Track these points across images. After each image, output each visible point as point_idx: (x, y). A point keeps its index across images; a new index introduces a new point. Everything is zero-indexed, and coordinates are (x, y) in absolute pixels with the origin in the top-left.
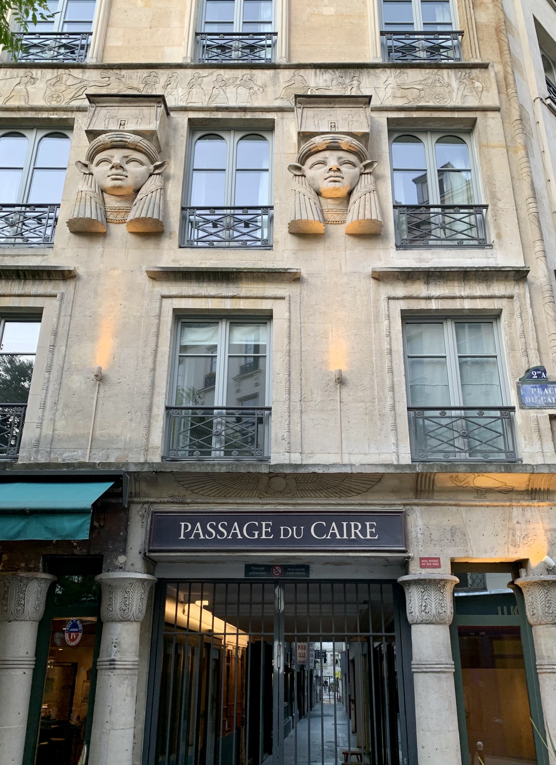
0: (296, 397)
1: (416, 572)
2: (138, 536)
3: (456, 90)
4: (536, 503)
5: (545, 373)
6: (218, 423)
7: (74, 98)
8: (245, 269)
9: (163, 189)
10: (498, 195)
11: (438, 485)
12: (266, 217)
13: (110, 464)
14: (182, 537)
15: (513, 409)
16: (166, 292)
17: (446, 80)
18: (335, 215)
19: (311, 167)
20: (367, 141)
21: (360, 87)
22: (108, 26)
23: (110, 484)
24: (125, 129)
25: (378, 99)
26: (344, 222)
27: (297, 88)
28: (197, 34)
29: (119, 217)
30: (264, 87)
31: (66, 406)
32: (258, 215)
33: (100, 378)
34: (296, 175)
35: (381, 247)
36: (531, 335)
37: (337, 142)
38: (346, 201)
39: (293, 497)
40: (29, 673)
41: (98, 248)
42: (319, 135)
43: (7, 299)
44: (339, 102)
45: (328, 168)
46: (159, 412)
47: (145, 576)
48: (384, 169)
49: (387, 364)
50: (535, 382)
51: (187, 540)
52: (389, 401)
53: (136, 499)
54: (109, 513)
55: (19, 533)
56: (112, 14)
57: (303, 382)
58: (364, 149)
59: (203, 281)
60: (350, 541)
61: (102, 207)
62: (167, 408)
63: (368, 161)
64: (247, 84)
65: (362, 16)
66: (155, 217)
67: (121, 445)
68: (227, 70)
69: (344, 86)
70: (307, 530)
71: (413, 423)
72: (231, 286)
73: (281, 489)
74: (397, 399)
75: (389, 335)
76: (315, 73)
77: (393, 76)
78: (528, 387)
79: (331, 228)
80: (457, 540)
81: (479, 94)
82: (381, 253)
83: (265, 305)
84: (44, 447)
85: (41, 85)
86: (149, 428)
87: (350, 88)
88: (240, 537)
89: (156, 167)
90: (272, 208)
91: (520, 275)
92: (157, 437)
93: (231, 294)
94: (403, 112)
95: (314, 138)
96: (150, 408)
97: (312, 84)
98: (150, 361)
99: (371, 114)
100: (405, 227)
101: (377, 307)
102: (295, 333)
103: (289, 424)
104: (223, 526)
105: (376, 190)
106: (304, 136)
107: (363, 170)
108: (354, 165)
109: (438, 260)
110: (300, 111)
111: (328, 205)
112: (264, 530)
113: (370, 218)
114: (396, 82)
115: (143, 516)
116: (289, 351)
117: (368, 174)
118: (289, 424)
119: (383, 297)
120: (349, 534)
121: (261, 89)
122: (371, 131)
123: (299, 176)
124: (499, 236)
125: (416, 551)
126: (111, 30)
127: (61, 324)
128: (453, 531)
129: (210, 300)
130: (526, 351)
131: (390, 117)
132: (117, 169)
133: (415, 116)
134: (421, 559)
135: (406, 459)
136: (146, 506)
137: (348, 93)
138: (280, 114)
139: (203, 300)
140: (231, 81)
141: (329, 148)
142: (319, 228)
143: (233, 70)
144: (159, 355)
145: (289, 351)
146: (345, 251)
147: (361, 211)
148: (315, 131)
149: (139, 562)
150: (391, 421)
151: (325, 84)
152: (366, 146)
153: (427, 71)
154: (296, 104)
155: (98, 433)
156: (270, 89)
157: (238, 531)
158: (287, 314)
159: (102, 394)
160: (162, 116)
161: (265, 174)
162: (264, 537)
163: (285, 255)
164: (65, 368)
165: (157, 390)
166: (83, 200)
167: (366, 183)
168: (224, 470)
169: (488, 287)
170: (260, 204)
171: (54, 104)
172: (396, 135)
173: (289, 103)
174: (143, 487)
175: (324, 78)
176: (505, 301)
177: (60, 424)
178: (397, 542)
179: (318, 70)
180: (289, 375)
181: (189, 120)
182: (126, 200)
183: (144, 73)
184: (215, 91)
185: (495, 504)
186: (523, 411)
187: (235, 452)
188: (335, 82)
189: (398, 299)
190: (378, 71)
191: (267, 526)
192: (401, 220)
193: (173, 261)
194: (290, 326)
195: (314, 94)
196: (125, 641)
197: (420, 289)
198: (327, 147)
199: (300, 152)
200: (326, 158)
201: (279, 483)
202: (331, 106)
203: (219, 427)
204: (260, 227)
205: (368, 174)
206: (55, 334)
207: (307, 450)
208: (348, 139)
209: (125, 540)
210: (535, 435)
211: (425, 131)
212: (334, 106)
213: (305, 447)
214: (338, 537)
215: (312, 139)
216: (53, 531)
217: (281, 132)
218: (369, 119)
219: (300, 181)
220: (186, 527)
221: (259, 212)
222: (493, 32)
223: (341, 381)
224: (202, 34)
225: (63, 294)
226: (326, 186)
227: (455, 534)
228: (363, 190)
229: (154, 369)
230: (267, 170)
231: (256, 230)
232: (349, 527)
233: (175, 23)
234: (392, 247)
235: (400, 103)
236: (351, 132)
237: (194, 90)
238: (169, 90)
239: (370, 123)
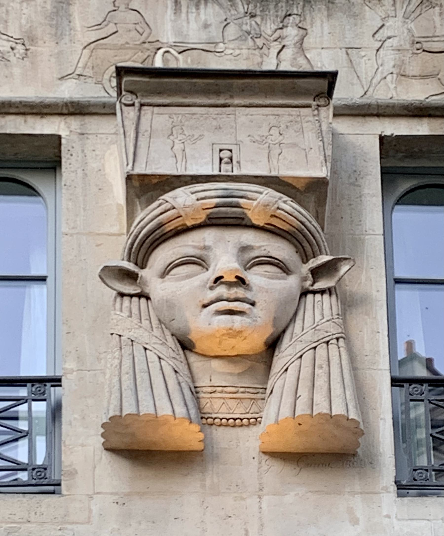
12: (40, 408)
20: (321, 202)
21: (305, 45)
25: (356, 81)
27: (122, 47)
32: (19, 401)
34: (122, 295)
37: (238, 206)
38: (261, 367)
42: (186, 184)
44: (243, 91)
45: (211, 275)
48: (368, 278)
58: (313, 225)
63: (324, 259)
69: (259, 42)
77: (400, 14)
79: (221, 435)
82: (358, 504)
87: (276, 47)
90: (56, 381)
94: (425, 121)
95: (171, 194)
97: (167, 36)
99: (334, 125)
100: (422, 434)
105: (344, 337)
106: (145, 187)
107: (309, 283)
108: (284, 269)
110: (131, 113)
111: (213, 375)
113: (326, 411)
114: (409, 30)
117: (322, 292)
121: (20, 49)
122: (334, 171)
123: (131, 296)
137: (270, 65)
138: (75, 123)
141: (214, 221)
142: (189, 436)
146: (260, 497)
147: (304, 393)
148: (175, 173)
151: (204, 36)
152: (319, 217)
154: (119, 93)
161: (36, 289)
163: (94, 508)
167: (318, 317)
170: (24, 373)
172: (405, 185)
173: (101, 90)
175: (203, 17)
192: (412, 415)
195: (173, 65)
198: (209, 217)
199: (134, 230)
200: (205, 248)
202: (221, 101)
204: (25, 435)
205: (322, 292)
208: (268, 195)
212: (229, 101)
215: (167, 196)
217: (80, 171)
218: (328, 138)
219: (135, 311)
221: (23, 392)
226: (205, 325)
228: (310, 337)
230: (42, 279)
231: (16, 440)
234: (386, 489)
236: (277, 177)
239: (329, 153)
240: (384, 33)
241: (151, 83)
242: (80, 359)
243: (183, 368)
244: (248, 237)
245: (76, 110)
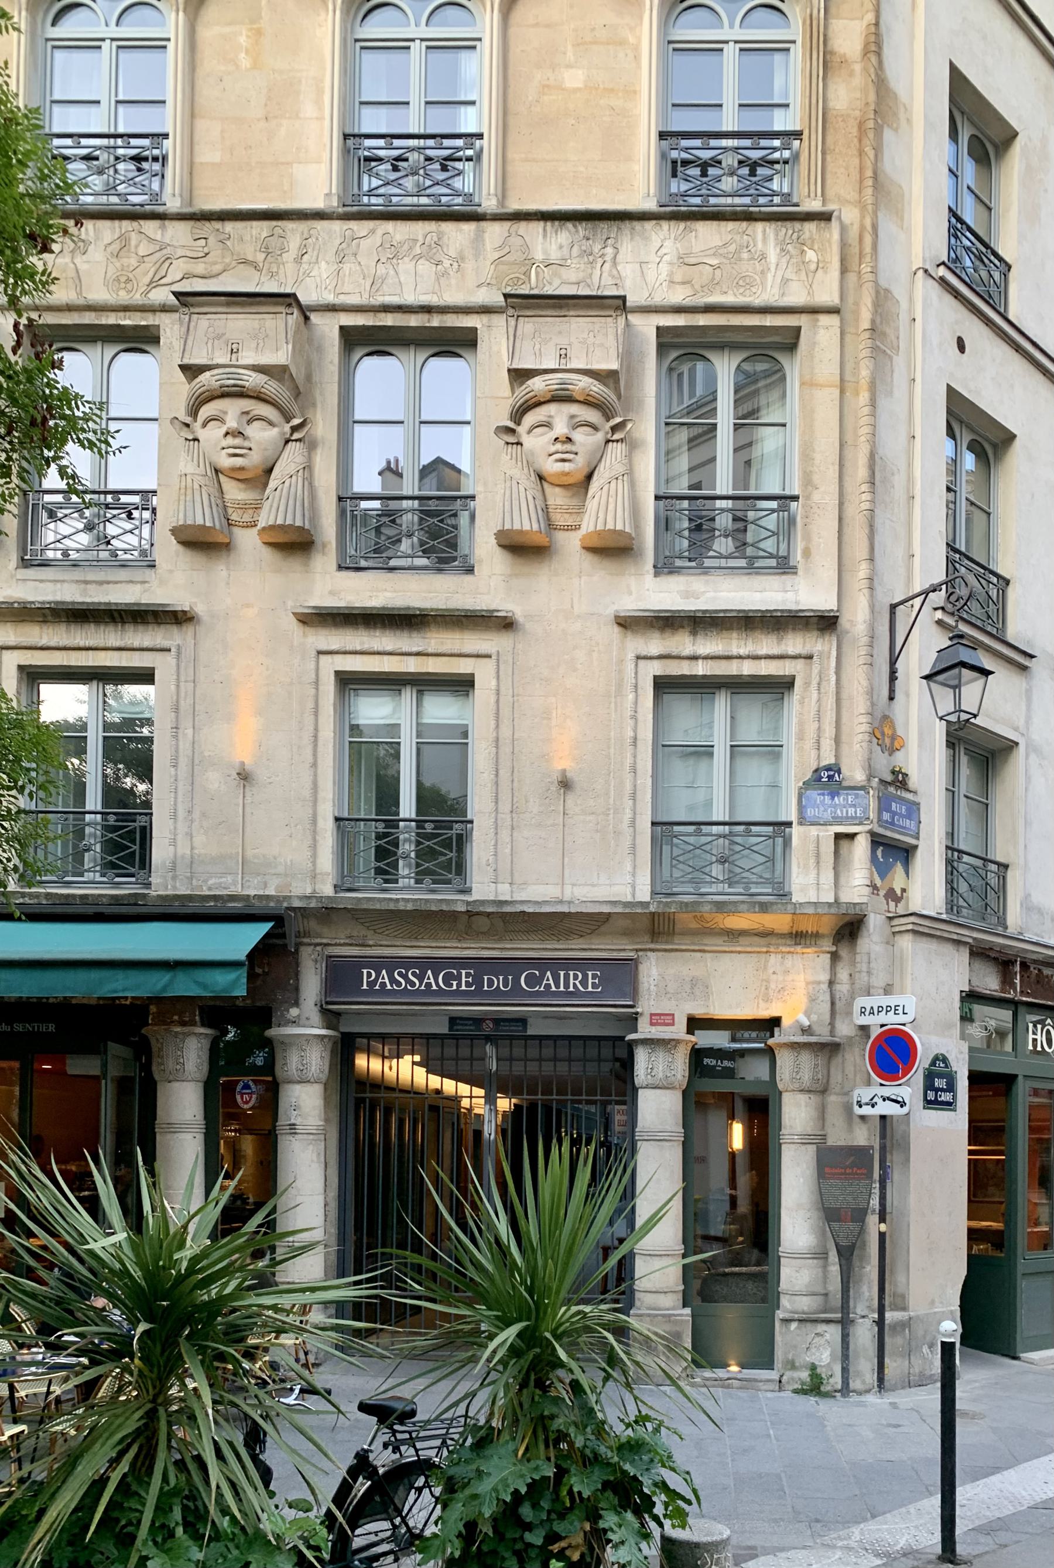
0: (505, 807)
1: (645, 1030)
2: (312, 985)
3: (773, 268)
4: (799, 949)
5: (839, 773)
6: (405, 840)
7: (153, 284)
8: (432, 610)
9: (308, 468)
10: (816, 478)
11: (678, 927)
13: (268, 897)
14: (365, 987)
15: (789, 824)
16: (324, 647)
17: (760, 245)
18: (567, 516)
22: (193, 116)
23: (270, 925)
24: (241, 362)
26: (577, 528)
27: (514, 263)
28: (346, 137)
29: (247, 518)
30: (460, 259)
31: (203, 815)
33: (245, 777)
35: (633, 571)
36: (829, 717)
39: (500, 940)
40: (200, 1138)
41: (220, 570)
43: (102, 654)
46: (327, 826)
47: (323, 1032)
49: (629, 761)
51: (371, 991)
52: (628, 814)
53: (306, 940)
54: (274, 958)
55: (165, 988)
56: (197, 88)
57: (516, 784)
59: (375, 627)
60: (568, 994)
61: (219, 501)
62: (337, 819)
64: (432, 253)
65: (631, 93)
66: (298, 523)
67: (281, 869)
68: (399, 223)
69: (591, 258)
70: (516, 981)
71: (656, 843)
72: (415, 634)
73: (485, 929)
74: (638, 811)
75: (634, 717)
76: (545, 230)
78: (813, 794)
80: (697, 992)
81: (811, 275)
82: (632, 582)
83: (462, 667)
84: (182, 871)
85: (96, 254)
86: (314, 847)
87: (600, 261)
88: (434, 987)
89: (294, 429)
91: (826, 623)
92: (327, 861)
93: (415, 649)
96: (314, 821)
98: (308, 751)
101: (620, 672)
102: (505, 711)
103: (496, 845)
104: (414, 974)
109: (712, 594)
111: (557, 498)
112: (464, 979)
115: (316, 961)
116: (497, 740)
118: (496, 845)
119: (631, 656)
120: (567, 986)
121: (455, 265)
124: (807, 553)
125: (647, 1005)
126: (201, 124)
127: (182, 695)
128: (694, 982)
129: (386, 658)
130: (818, 742)
132: (234, 436)
133: (701, 323)
134: (652, 1015)
135: (644, 894)
136: (319, 948)
138: (485, 318)
139: (377, 657)
140: (406, 247)
142: (542, 540)
143: (409, 223)
144: (320, 743)
145: (497, 740)
149: (315, 1016)
150: (627, 842)
151: (559, 255)
153: (731, 225)
155: (249, 853)
156: (469, 266)
157: (432, 980)
158: (494, 682)
159: (248, 800)
160: (297, 332)
162: (463, 988)
164: (196, 762)
165: (321, 794)
166: (189, 492)
168: (410, 907)
169: (780, 640)
171: (123, 297)
174: (313, 925)
177: (199, 839)
178: (624, 996)
179: (549, 224)
180: (497, 775)
181: (342, 328)
182: (255, 487)
183: (260, 228)
184: (381, 270)
185: (749, 949)
186: (802, 828)
187: (427, 880)
188: (575, 251)
189: (651, 658)
190: (649, 225)
191: (468, 975)
193: (332, 593)
194: (498, 701)
196: (306, 1104)
197: (684, 643)
201: (483, 923)
203: (407, 846)
206: (176, 709)
207: (518, 879)
209: (297, 989)
210: (812, 861)
211: (719, 347)
213: (516, 874)
214: (554, 989)
216: (205, 987)
220: (369, 975)
222: (855, 131)
223: (566, 784)
224: (354, 136)
225: (179, 647)
226: (551, 467)
227: (697, 986)
229: (314, 765)
232: (567, 977)
233: (309, 110)
235: (679, 296)
237: (346, 267)
238: (305, 266)
240: (663, 251)
241: (524, 303)
242: (485, 484)
243: (539, 495)
245: (486, 310)
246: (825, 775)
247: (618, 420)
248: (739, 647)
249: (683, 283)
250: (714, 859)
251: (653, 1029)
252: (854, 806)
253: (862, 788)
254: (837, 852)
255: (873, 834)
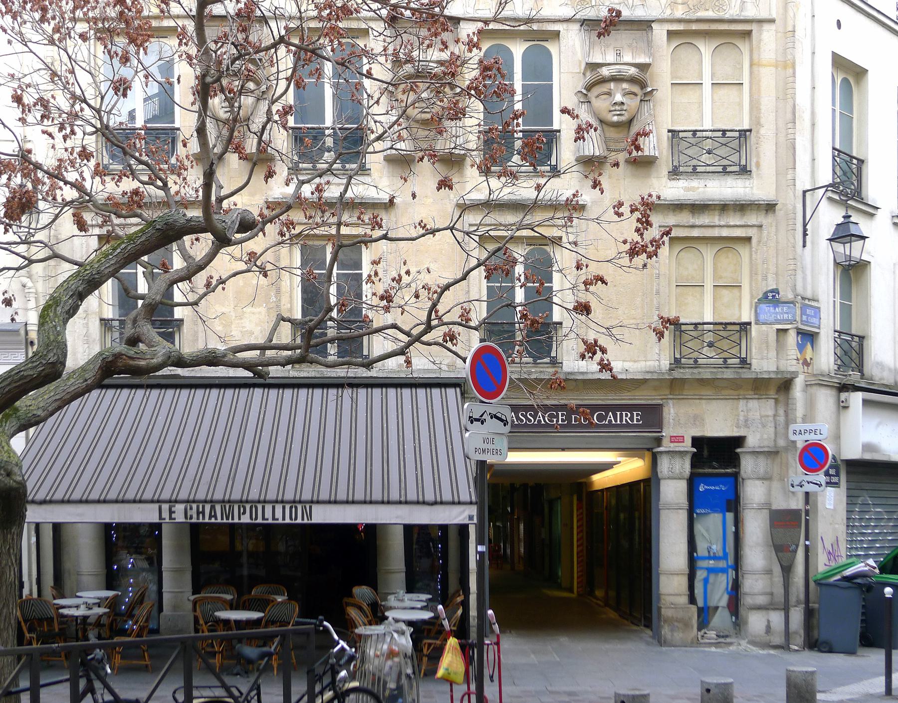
10: (763, 121)
15: (749, 324)
19: (597, 97)
50: (770, 302)
60: (621, 426)
78: (763, 306)
80: (697, 423)
91: (770, 207)
104: (530, 415)
108: (636, 95)
120: (621, 420)
124: (758, 165)
131: (670, 29)
176: (755, 230)
191: (562, 415)
227: (697, 419)
244: (625, 85)
246: (770, 295)
247: (649, 89)
248: (719, 220)
249: (683, 4)
250: (705, 344)
251: (672, 445)
252: (787, 313)
253: (792, 302)
254: (778, 341)
255: (797, 329)
